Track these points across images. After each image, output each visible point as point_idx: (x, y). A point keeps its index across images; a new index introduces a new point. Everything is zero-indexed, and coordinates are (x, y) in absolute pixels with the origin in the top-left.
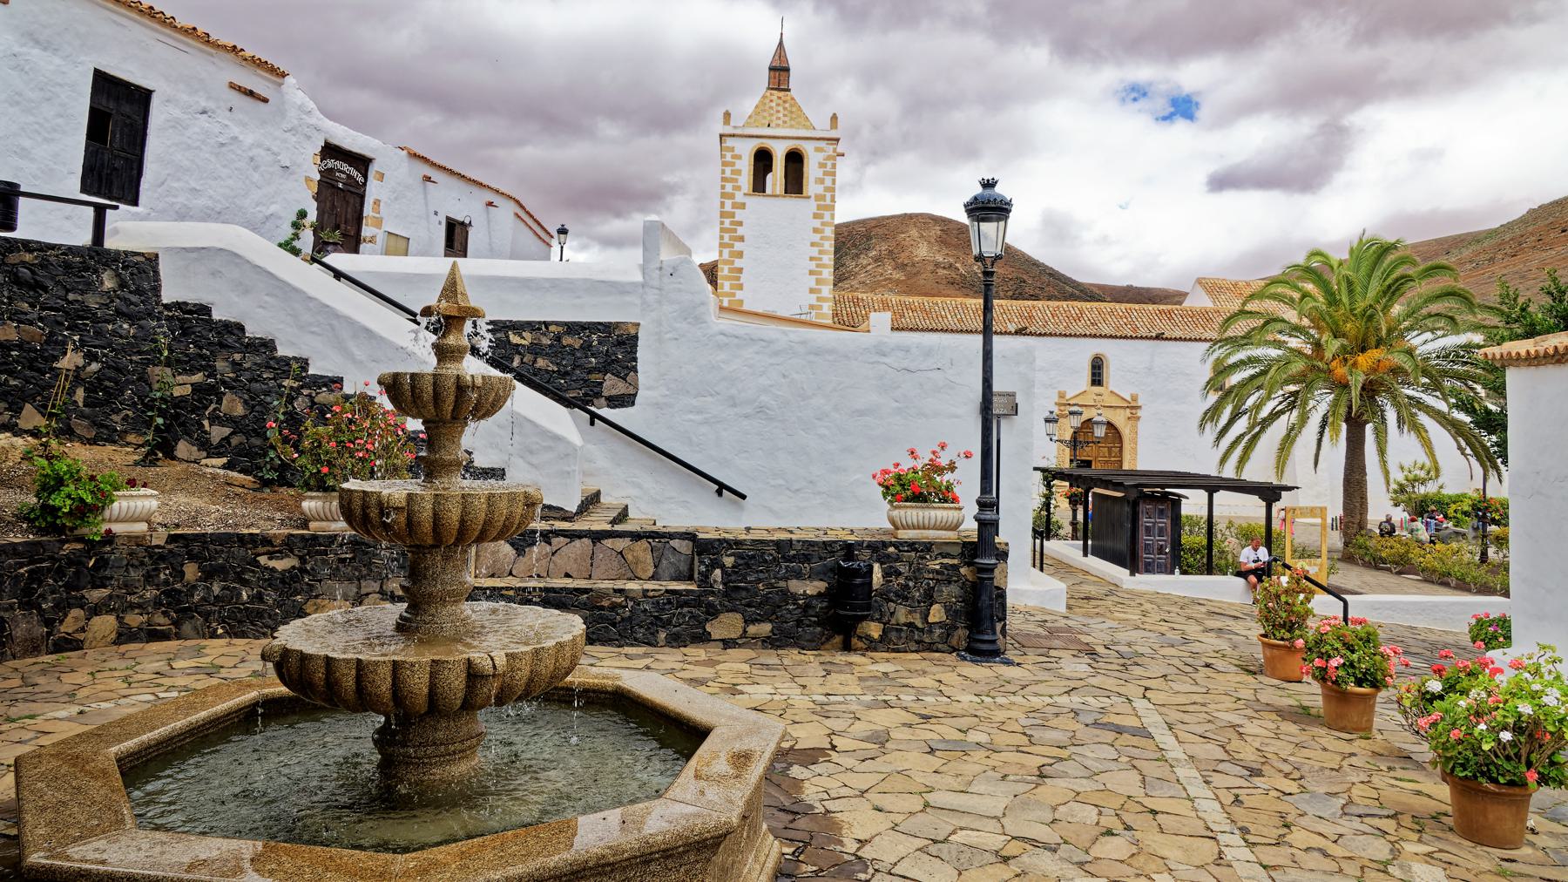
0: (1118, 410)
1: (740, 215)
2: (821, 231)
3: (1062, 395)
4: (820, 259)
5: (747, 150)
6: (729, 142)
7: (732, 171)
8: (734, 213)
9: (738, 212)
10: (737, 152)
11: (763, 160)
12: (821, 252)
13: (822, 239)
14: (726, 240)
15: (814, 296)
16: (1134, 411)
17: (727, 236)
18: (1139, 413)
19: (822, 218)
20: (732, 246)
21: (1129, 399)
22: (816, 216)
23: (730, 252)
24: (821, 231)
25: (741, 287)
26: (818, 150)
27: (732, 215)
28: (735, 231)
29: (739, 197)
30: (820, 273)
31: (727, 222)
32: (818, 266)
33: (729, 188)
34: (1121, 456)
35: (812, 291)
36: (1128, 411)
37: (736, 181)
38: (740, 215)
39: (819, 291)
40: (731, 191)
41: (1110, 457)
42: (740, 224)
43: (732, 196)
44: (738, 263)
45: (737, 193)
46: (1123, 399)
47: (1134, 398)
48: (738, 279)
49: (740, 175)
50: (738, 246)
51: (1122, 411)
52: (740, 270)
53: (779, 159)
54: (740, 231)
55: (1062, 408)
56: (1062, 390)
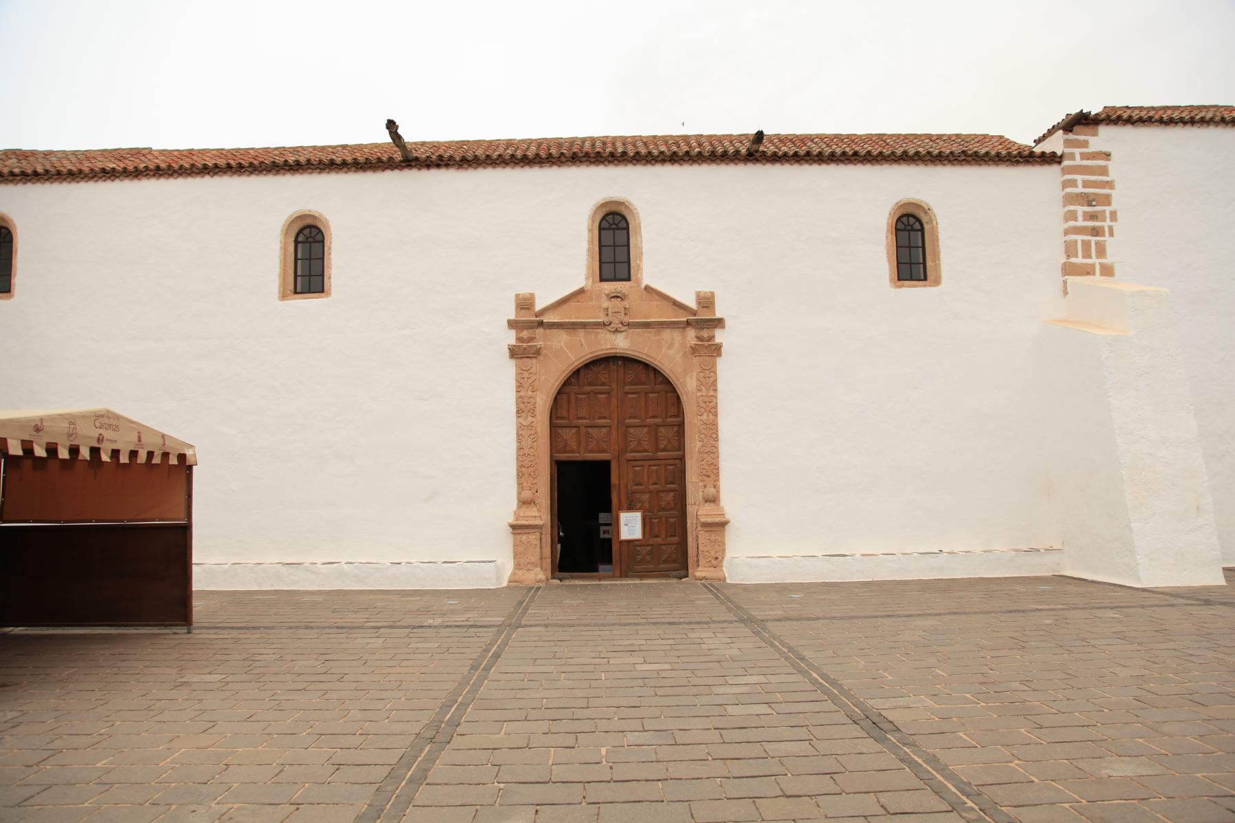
0: (667, 334)
3: (525, 304)
16: (705, 334)
18: (720, 336)
21: (692, 303)
34: (681, 447)
36: (691, 334)
41: (657, 449)
46: (676, 304)
47: (707, 301)
51: (676, 335)
55: (525, 334)
56: (524, 291)
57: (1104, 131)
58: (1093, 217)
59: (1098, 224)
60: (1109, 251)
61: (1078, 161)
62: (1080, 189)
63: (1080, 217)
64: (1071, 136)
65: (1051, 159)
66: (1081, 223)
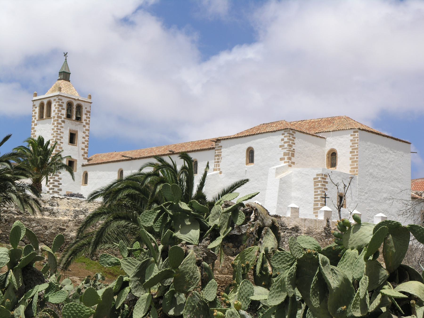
5: (38, 104)
6: (35, 103)
9: (35, 127)
10: (36, 106)
26: (54, 100)
29: (36, 122)
37: (35, 116)
57: (222, 142)
58: (218, 159)
59: (219, 160)
60: (220, 165)
61: (217, 148)
63: (216, 159)
64: (216, 143)
65: (213, 148)
66: (216, 161)
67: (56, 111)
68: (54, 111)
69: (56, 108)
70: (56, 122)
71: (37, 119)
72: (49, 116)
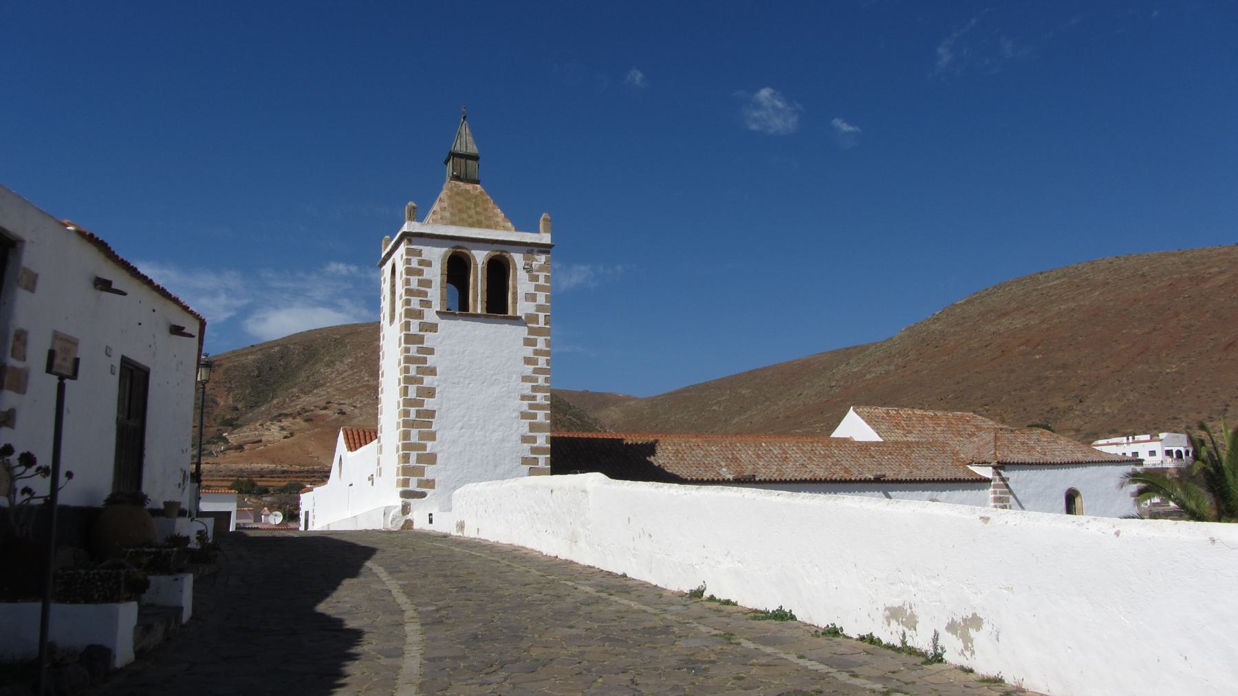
1: (430, 339)
2: (535, 362)
4: (534, 398)
7: (419, 281)
8: (422, 337)
9: (428, 335)
11: (457, 269)
12: (534, 389)
13: (536, 371)
14: (413, 372)
15: (527, 446)
17: (413, 367)
19: (536, 345)
20: (421, 381)
22: (528, 342)
23: (418, 389)
24: (535, 362)
25: (432, 437)
27: (420, 340)
28: (425, 361)
29: (430, 316)
30: (534, 416)
31: (414, 348)
32: (531, 407)
33: (415, 303)
35: (525, 439)
37: (426, 294)
38: (430, 339)
39: (534, 439)
40: (418, 308)
42: (431, 351)
43: (419, 315)
44: (429, 404)
45: (426, 310)
48: (430, 425)
49: (430, 287)
50: (428, 381)
52: (432, 414)
53: (480, 267)
54: (431, 360)
62: (998, 495)
67: (541, 298)
68: (531, 297)
69: (538, 288)
70: (543, 338)
71: (437, 306)
72: (497, 305)
